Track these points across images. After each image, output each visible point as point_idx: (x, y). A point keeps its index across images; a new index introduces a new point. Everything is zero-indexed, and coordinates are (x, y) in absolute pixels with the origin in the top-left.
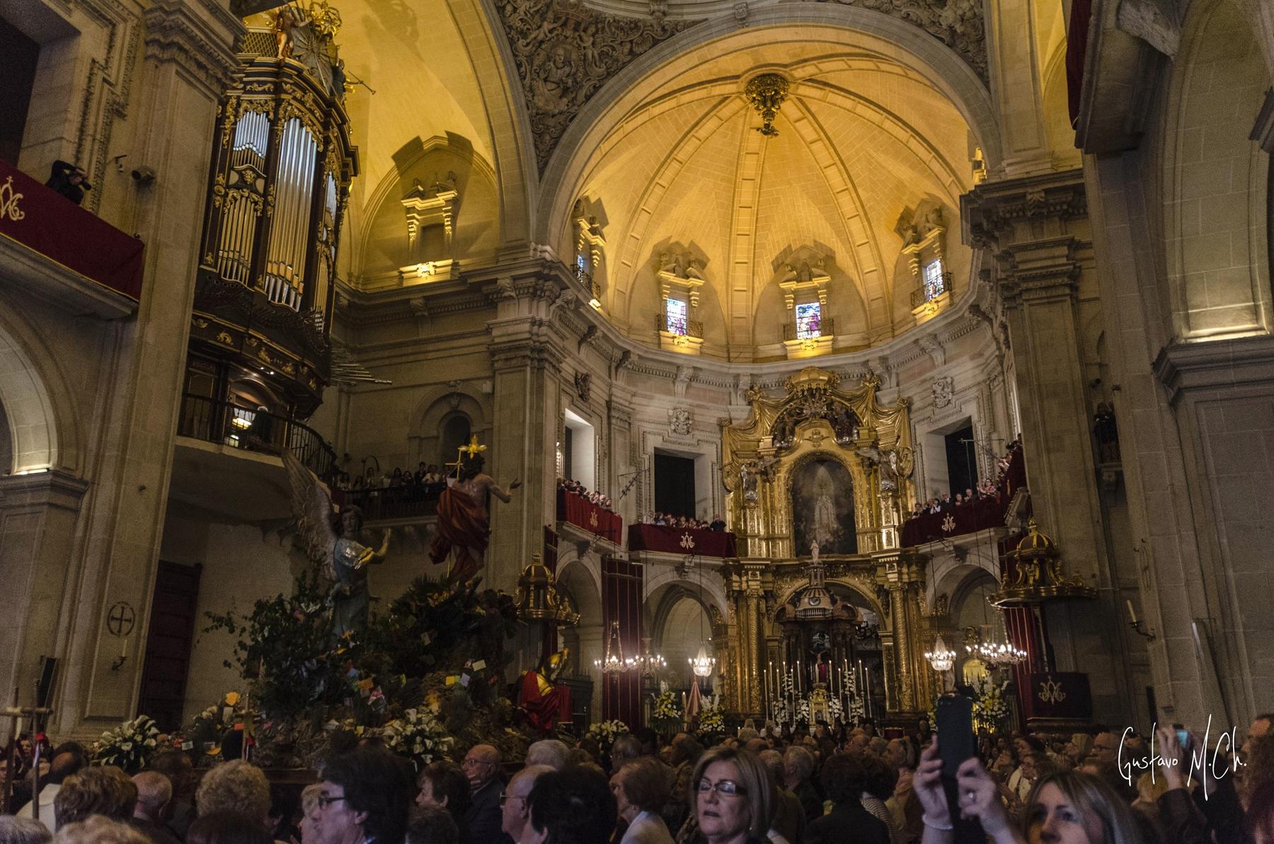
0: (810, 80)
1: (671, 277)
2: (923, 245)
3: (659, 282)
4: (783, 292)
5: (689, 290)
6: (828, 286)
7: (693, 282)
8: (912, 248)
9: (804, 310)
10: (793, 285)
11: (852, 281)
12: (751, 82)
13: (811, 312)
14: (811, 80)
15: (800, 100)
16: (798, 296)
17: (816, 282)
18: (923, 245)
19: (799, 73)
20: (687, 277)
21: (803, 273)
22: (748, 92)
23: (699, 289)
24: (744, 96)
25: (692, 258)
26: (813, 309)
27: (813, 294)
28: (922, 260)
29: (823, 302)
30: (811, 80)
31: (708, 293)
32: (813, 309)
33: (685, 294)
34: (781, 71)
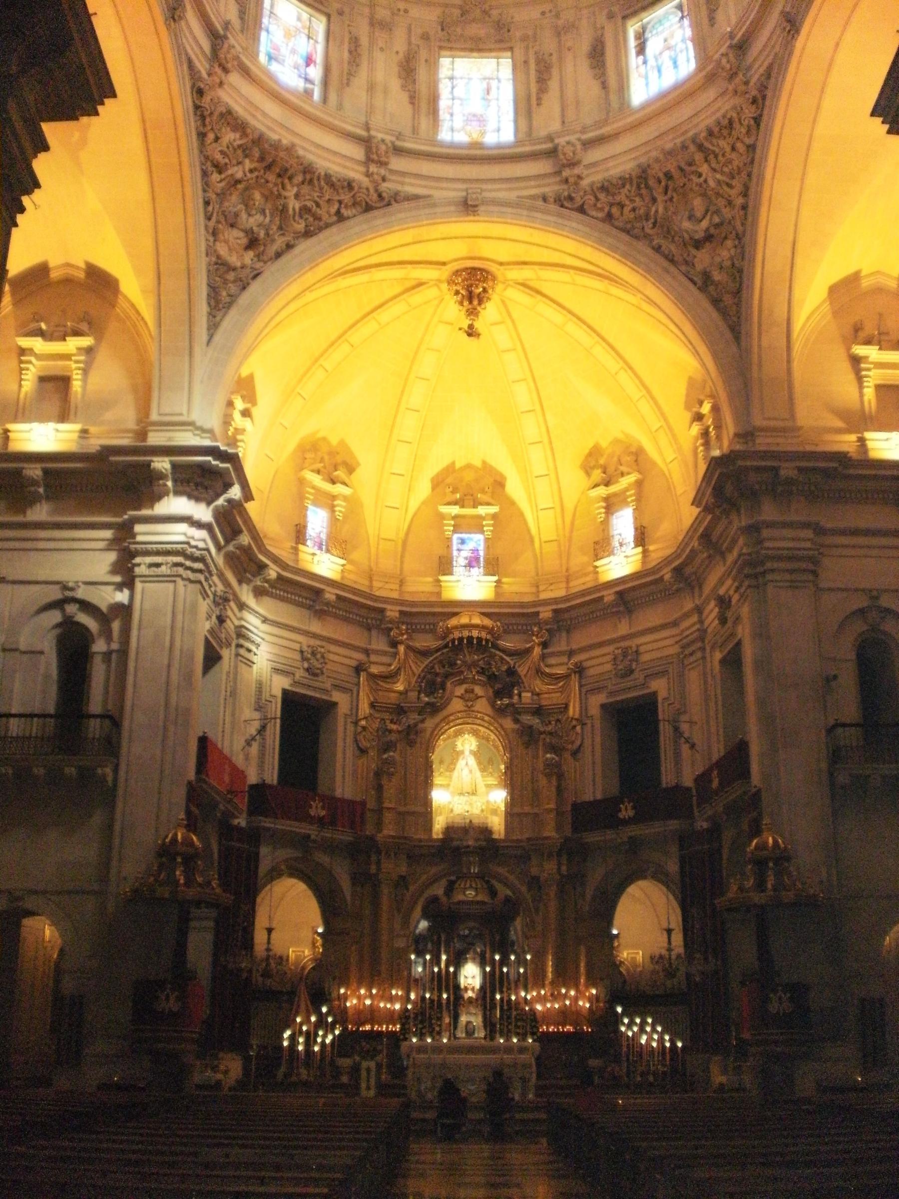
0: (524, 285)
1: (317, 480)
2: (613, 489)
3: (301, 482)
4: (442, 517)
5: (334, 497)
6: (494, 517)
7: (339, 489)
8: (602, 491)
9: (463, 542)
10: (455, 510)
11: (522, 515)
12: (457, 273)
13: (471, 545)
14: (524, 285)
15: (503, 302)
16: (460, 525)
17: (482, 510)
18: (613, 489)
19: (515, 274)
20: (333, 482)
21: (468, 499)
22: (450, 282)
23: (345, 498)
24: (445, 286)
25: (339, 459)
26: (476, 541)
27: (476, 525)
28: (611, 505)
29: (488, 534)
30: (524, 285)
31: (353, 503)
32: (476, 541)
33: (328, 502)
34: (493, 268)
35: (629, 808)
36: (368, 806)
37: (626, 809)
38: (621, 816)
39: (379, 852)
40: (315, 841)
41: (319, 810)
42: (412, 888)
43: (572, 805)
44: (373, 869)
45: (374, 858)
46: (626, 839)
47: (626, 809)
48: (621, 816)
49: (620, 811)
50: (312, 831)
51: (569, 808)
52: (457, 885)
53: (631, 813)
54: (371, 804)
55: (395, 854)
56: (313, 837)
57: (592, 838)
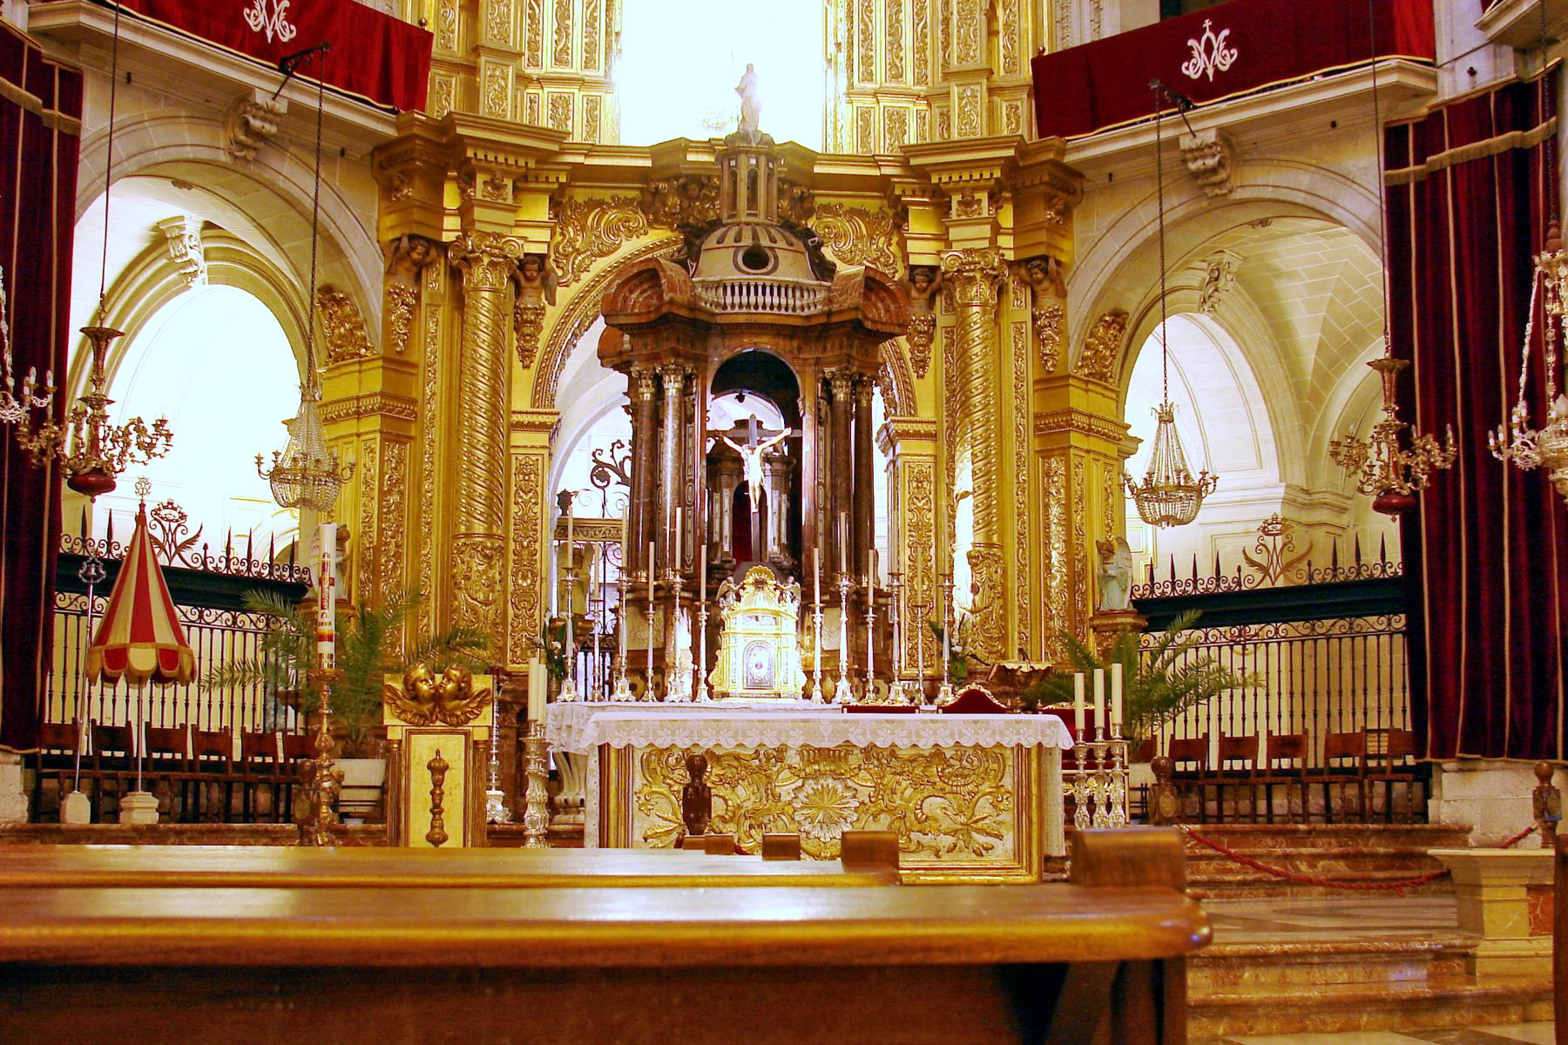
35: (1219, 43)
36: (436, 50)
37: (1209, 49)
38: (1191, 71)
39: (467, 180)
40: (269, 114)
41: (279, 22)
42: (564, 295)
43: (1034, 62)
44: (450, 228)
45: (451, 199)
46: (1211, 137)
47: (1209, 49)
48: (1191, 71)
49: (1187, 54)
50: (261, 81)
51: (1026, 73)
52: (711, 241)
53: (1225, 59)
54: (449, 42)
55: (516, 190)
56: (261, 98)
57: (1089, 147)
